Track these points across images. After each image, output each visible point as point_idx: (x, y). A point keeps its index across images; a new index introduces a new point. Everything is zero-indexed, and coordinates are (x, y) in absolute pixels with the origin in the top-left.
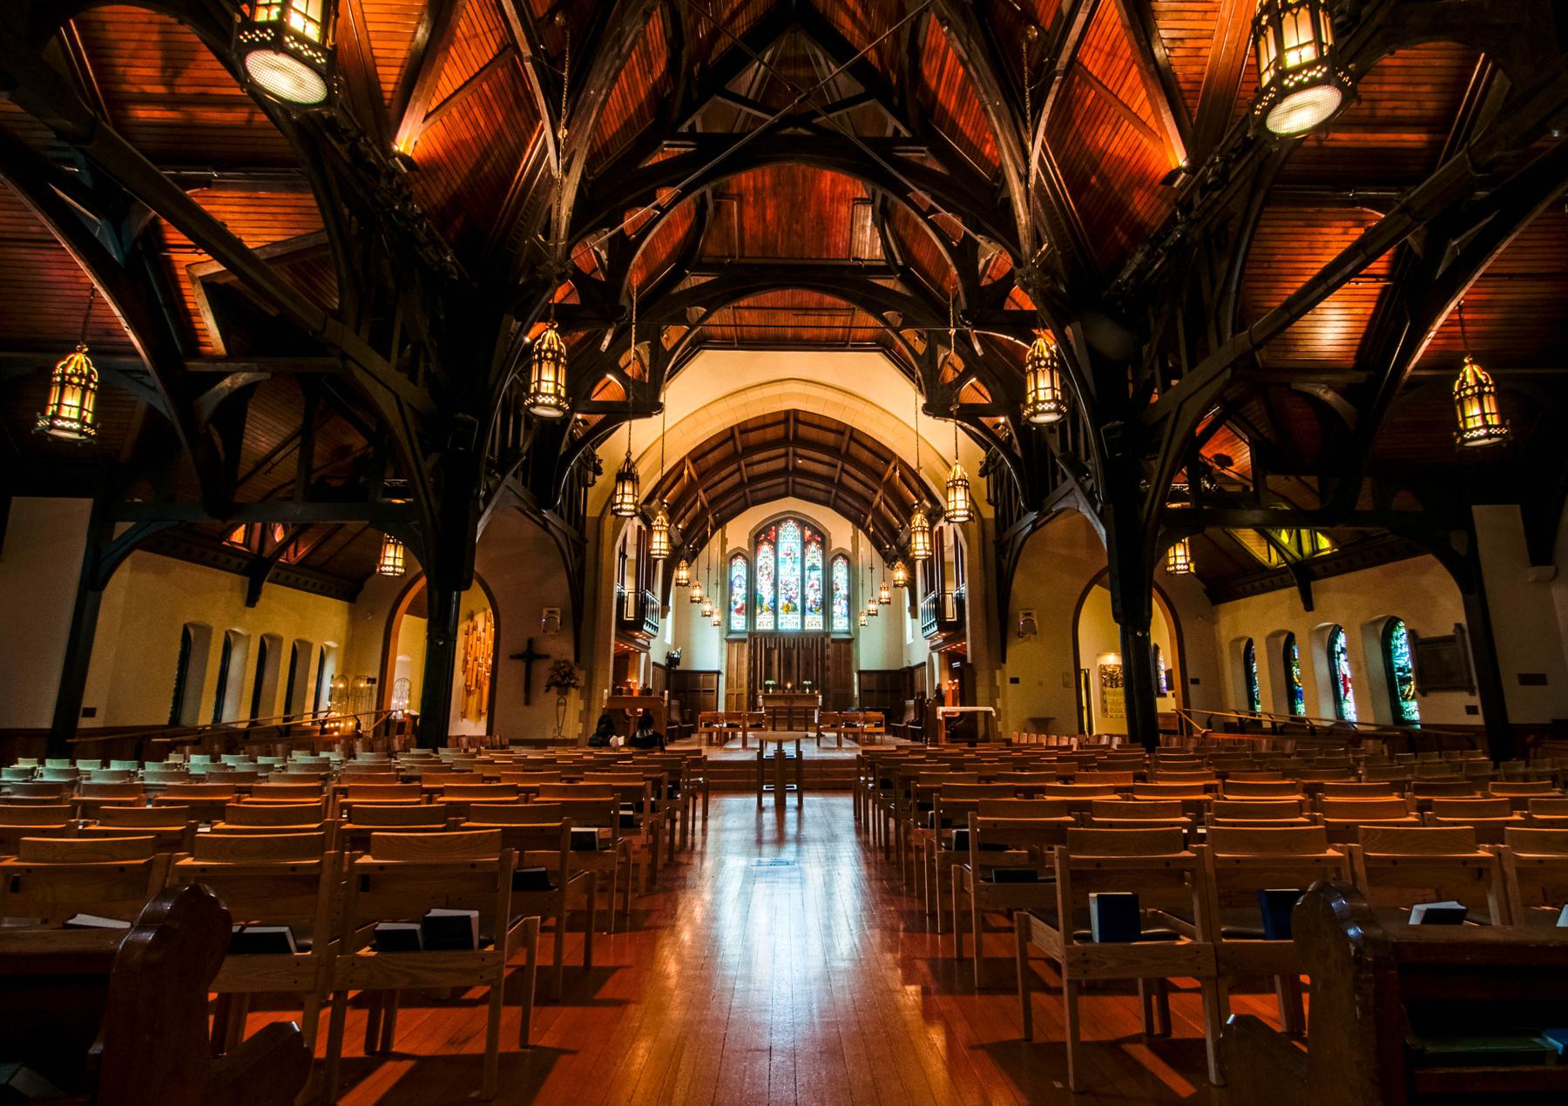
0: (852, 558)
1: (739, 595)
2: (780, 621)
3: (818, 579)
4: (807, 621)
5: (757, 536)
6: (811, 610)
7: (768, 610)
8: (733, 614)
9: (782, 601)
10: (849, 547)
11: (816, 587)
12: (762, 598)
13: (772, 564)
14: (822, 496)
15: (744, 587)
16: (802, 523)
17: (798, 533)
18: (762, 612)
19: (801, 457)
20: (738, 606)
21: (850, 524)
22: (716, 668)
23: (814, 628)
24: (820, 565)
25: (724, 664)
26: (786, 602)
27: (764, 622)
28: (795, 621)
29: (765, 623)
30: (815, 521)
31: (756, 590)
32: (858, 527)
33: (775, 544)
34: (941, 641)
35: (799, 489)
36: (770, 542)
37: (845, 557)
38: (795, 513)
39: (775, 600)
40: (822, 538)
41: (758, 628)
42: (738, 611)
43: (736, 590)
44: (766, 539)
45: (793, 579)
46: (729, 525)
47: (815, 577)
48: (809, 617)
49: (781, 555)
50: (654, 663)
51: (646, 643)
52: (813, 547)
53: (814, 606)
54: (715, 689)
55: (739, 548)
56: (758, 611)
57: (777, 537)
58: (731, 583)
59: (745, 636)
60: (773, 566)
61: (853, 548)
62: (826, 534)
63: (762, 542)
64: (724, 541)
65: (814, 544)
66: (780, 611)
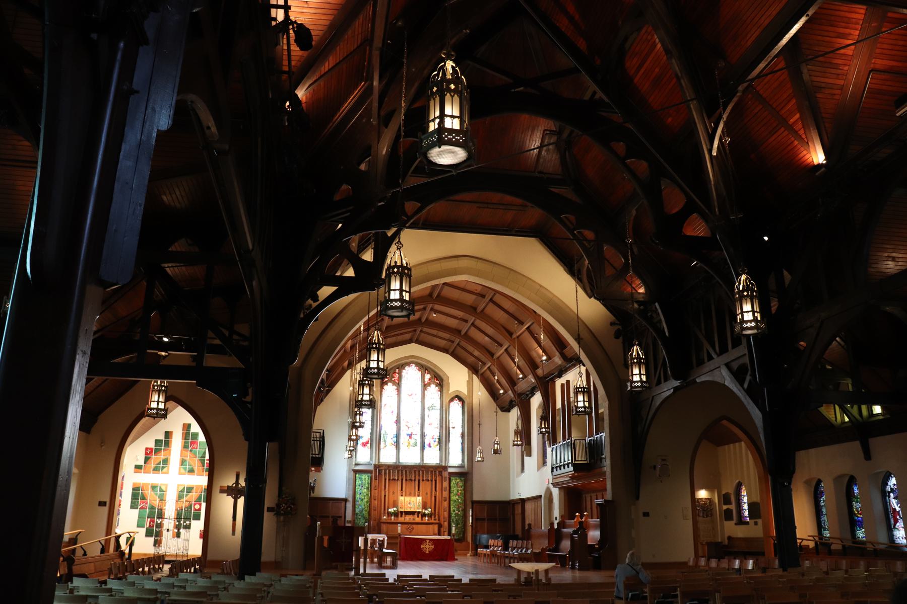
0: (466, 402)
6: (430, 446)
9: (404, 439)
10: (464, 390)
14: (442, 343)
16: (424, 368)
19: (436, 312)
21: (467, 369)
22: (343, 496)
25: (351, 493)
27: (388, 457)
32: (473, 373)
33: (398, 385)
34: (568, 479)
35: (424, 337)
36: (394, 383)
37: (460, 399)
38: (418, 358)
39: (398, 436)
40: (439, 380)
44: (390, 381)
47: (433, 418)
54: (343, 517)
59: (372, 468)
61: (468, 391)
62: (444, 378)
63: (386, 383)
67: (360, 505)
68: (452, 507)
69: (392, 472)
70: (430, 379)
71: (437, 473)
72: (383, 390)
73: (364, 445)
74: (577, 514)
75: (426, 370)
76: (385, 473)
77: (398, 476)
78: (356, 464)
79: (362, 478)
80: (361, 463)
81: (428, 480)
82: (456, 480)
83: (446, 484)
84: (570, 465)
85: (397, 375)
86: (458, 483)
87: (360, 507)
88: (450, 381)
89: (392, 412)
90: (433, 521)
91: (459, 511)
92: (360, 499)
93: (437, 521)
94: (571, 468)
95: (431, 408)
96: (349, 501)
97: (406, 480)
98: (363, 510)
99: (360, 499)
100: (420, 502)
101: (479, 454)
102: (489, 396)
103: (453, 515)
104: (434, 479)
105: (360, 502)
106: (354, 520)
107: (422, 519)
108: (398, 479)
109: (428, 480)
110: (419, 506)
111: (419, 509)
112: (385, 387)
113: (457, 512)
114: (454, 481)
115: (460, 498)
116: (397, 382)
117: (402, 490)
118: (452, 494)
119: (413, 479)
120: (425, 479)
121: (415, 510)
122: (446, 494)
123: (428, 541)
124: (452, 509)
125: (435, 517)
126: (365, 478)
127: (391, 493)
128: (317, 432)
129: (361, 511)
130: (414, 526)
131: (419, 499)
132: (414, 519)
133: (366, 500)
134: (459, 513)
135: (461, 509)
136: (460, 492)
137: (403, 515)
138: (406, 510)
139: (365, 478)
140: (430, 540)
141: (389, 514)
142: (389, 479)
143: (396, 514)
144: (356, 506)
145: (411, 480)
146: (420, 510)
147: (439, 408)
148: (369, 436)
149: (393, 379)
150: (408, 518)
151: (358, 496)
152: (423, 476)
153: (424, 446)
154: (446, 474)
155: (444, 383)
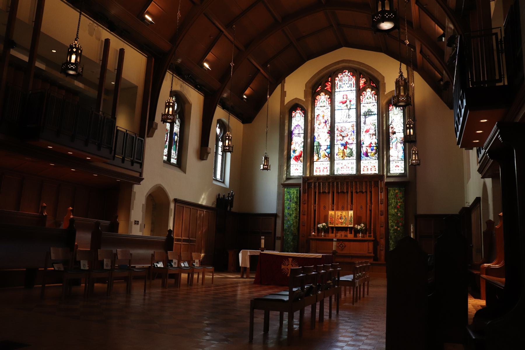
2: (336, 167)
6: (367, 155)
8: (293, 161)
9: (338, 148)
12: (319, 145)
17: (354, 80)
20: (297, 154)
22: (274, 211)
23: (369, 172)
24: (375, 110)
25: (281, 208)
29: (322, 169)
33: (331, 95)
39: (332, 146)
42: (297, 159)
46: (287, 79)
48: (364, 162)
49: (337, 105)
50: (176, 201)
51: (137, 175)
52: (369, 93)
55: (296, 99)
56: (316, 158)
57: (333, 86)
58: (291, 133)
62: (380, 79)
64: (283, 94)
65: (369, 90)
66: (336, 156)
67: (288, 221)
68: (390, 221)
69: (322, 185)
70: (365, 83)
71: (373, 184)
72: (316, 101)
73: (297, 159)
75: (360, 74)
76: (315, 186)
77: (329, 189)
78: (288, 179)
79: (290, 192)
80: (293, 177)
81: (363, 192)
82: (395, 190)
83: (382, 196)
85: (329, 83)
86: (397, 193)
87: (288, 223)
90: (367, 238)
91: (398, 227)
92: (288, 214)
93: (372, 238)
95: (369, 113)
96: (279, 217)
97: (338, 193)
98: (291, 226)
99: (288, 214)
100: (351, 217)
101: (414, 156)
102: (434, 92)
103: (391, 231)
104: (368, 192)
105: (289, 218)
106: (284, 237)
107: (355, 236)
108: (329, 193)
109: (363, 192)
110: (351, 221)
111: (350, 224)
112: (318, 97)
113: (396, 227)
114: (392, 192)
115: (400, 211)
116: (329, 90)
117: (333, 203)
118: (390, 207)
119: (345, 191)
120: (358, 191)
121: (347, 226)
122: (382, 207)
123: (290, 260)
124: (390, 225)
125: (370, 233)
126: (294, 191)
127: (322, 208)
129: (289, 227)
130: (347, 243)
131: (351, 213)
132: (346, 236)
133: (294, 215)
134: (399, 229)
135: (400, 224)
136: (399, 204)
137: (334, 232)
138: (336, 226)
139: (294, 191)
140: (294, 258)
141: (319, 230)
142: (319, 193)
143: (326, 230)
144: (285, 222)
145: (344, 193)
146: (352, 226)
148: (302, 149)
150: (340, 235)
151: (286, 211)
152: (356, 188)
153: (361, 156)
154: (381, 185)
155: (381, 84)
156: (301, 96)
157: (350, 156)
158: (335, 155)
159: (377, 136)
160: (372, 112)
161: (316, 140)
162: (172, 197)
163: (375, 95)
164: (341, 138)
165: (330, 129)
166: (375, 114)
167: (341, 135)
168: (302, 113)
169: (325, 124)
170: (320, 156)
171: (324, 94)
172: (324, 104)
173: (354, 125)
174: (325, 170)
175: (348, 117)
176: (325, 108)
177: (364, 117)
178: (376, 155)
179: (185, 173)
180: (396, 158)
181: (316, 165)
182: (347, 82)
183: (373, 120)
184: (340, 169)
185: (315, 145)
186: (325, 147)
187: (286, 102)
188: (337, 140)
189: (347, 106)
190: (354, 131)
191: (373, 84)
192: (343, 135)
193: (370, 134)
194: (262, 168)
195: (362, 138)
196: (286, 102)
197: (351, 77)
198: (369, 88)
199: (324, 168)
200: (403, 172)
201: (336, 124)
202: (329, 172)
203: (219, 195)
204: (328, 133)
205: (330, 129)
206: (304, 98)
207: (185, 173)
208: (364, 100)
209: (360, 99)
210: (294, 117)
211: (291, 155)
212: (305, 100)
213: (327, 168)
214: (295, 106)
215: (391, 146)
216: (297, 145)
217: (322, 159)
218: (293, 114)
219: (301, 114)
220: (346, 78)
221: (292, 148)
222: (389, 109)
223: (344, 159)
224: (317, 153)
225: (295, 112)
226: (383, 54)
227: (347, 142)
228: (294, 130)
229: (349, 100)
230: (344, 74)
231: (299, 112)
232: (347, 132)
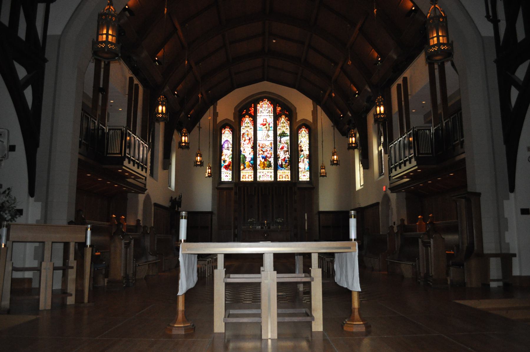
1: (227, 155)
3: (287, 144)
4: (278, 174)
5: (241, 111)
6: (281, 166)
7: (249, 166)
8: (223, 170)
9: (259, 160)
10: (310, 118)
11: (285, 149)
12: (245, 157)
13: (252, 132)
15: (231, 149)
16: (275, 101)
18: (244, 168)
20: (227, 164)
21: (311, 101)
22: (210, 210)
23: (284, 179)
24: (288, 132)
26: (263, 160)
27: (247, 175)
28: (269, 174)
29: (247, 176)
30: (285, 99)
31: (240, 151)
36: (250, 116)
39: (255, 159)
41: (242, 180)
42: (227, 167)
43: (225, 151)
44: (247, 113)
45: (268, 143)
46: (219, 102)
48: (280, 172)
50: (155, 205)
52: (283, 119)
53: (284, 163)
55: (227, 119)
56: (242, 167)
58: (221, 147)
60: (252, 133)
61: (313, 119)
63: (244, 116)
64: (215, 115)
65: (283, 116)
66: (258, 167)
70: (280, 111)
74: (419, 217)
84: (413, 160)
88: (297, 112)
89: (250, 139)
94: (414, 163)
95: (283, 135)
112: (244, 119)
116: (253, 114)
128: (118, 129)
147: (289, 135)
148: (231, 160)
149: (249, 112)
153: (277, 167)
156: (231, 118)
157: (269, 166)
158: (258, 165)
159: (289, 152)
160: (286, 134)
161: (242, 153)
162: (153, 203)
163: (288, 121)
164: (262, 152)
165: (253, 145)
166: (288, 136)
167: (262, 150)
168: (230, 131)
169: (249, 141)
170: (245, 166)
171: (248, 117)
172: (249, 125)
173: (272, 143)
174: (250, 177)
175: (267, 136)
176: (249, 128)
177: (279, 137)
178: (288, 167)
179: (157, 181)
180: (304, 170)
181: (242, 173)
182: (266, 109)
183: (286, 139)
184: (262, 176)
185: (241, 157)
186: (250, 159)
187: (218, 122)
188: (259, 154)
189: (266, 128)
190: (272, 147)
191: (286, 112)
192: (263, 151)
193: (284, 151)
194: (207, 176)
195: (278, 153)
196: (218, 122)
197: (270, 105)
198: (284, 115)
199: (249, 175)
200: (308, 180)
201: (258, 142)
202: (253, 178)
203: (172, 198)
204: (252, 148)
205: (253, 145)
206: (234, 119)
207: (157, 181)
208: (279, 124)
209: (277, 123)
210: (223, 133)
211: (222, 165)
212: (234, 121)
213: (251, 175)
214: (225, 125)
215: (300, 160)
216: (227, 156)
217: (247, 169)
218: (223, 131)
219: (229, 131)
220: (265, 106)
221: (222, 159)
222: (299, 132)
223: (264, 169)
224: (243, 164)
225: (225, 129)
226: (296, 90)
227: (267, 156)
228: (223, 144)
229: (268, 123)
230: (264, 102)
231: (228, 130)
232: (267, 148)
